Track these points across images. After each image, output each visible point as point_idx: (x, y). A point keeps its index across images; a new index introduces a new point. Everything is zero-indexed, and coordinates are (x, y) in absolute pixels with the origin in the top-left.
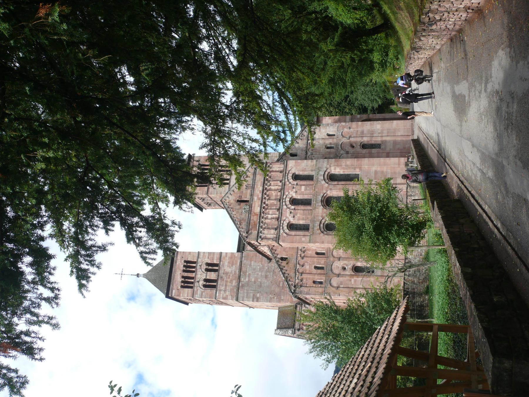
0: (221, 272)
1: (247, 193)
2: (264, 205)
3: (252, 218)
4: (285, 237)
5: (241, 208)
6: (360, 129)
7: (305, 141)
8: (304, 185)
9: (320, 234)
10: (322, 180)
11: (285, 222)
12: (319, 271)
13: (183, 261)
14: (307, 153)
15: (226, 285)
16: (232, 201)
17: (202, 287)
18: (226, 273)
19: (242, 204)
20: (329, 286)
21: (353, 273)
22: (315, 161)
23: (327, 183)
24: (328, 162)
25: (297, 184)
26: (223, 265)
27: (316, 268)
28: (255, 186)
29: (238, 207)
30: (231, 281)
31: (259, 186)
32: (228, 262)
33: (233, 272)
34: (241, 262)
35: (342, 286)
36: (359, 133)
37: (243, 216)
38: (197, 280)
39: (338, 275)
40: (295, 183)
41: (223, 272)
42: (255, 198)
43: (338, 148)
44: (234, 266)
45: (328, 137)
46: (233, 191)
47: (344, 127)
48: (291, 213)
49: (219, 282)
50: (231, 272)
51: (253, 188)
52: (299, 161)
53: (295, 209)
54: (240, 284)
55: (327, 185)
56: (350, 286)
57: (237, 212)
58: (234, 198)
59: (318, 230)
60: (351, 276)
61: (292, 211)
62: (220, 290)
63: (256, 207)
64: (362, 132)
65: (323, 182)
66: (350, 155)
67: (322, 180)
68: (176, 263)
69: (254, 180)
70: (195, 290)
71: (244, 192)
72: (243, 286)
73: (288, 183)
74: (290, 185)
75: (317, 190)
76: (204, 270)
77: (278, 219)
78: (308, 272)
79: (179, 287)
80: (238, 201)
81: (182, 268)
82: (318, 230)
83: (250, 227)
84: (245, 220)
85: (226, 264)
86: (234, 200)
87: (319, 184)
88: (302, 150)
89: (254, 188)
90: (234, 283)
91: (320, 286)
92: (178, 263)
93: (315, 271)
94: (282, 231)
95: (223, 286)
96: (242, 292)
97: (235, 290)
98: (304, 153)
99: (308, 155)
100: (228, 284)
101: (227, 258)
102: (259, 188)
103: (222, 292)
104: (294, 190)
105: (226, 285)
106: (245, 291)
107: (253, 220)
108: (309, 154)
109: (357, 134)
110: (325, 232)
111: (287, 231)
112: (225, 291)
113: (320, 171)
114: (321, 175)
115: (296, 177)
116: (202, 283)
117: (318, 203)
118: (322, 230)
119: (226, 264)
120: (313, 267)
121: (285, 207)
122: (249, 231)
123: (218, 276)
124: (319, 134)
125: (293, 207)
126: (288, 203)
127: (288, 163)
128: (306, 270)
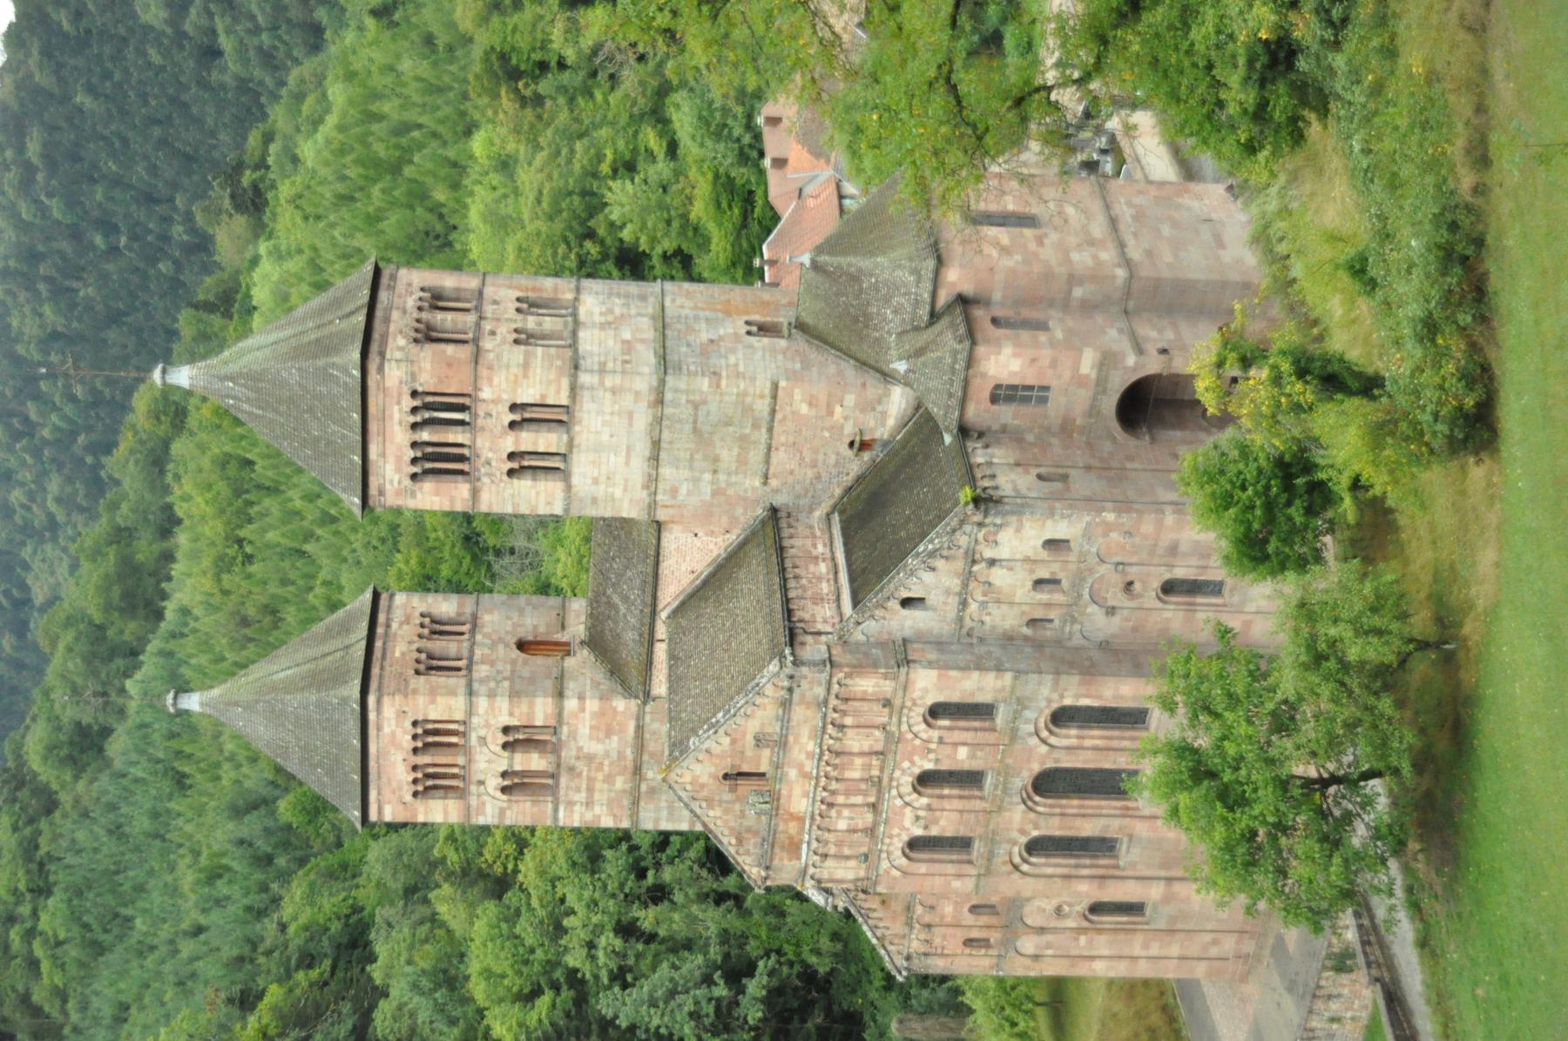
0: (568, 754)
1: (759, 757)
2: (825, 794)
3: (781, 827)
4: (895, 878)
5: (738, 799)
6: (1167, 538)
7: (960, 565)
8: (965, 744)
9: (1009, 873)
10: (1030, 735)
11: (895, 840)
12: (984, 920)
13: (408, 724)
14: (964, 604)
15: (590, 790)
16: (704, 779)
17: (499, 794)
18: (590, 758)
19: (745, 786)
20: (1012, 954)
21: (1085, 924)
22: (1008, 676)
23: (1044, 741)
24: (1056, 683)
25: (941, 741)
26: (573, 735)
27: (974, 909)
28: (791, 738)
29: (727, 796)
30: (609, 779)
31: (804, 739)
32: (592, 728)
33: (614, 755)
34: (640, 729)
35: (1050, 952)
36: (1160, 551)
37: (747, 823)
38: (476, 777)
39: (1042, 930)
40: (935, 734)
41: (574, 753)
42: (793, 773)
43: (1080, 596)
44: (615, 738)
45: (1044, 554)
46: (708, 751)
47: (1108, 528)
48: (918, 818)
49: (563, 781)
50: (607, 754)
51: (782, 743)
52: (953, 673)
53: (929, 808)
54: (644, 787)
55: (1044, 749)
56: (1075, 952)
57: (727, 811)
58: (713, 769)
59: (1004, 863)
60: (1080, 931)
61: (922, 813)
62: (571, 804)
63: (794, 799)
64: (1173, 550)
65: (1034, 741)
66: (1116, 620)
67: (1030, 735)
68: (379, 729)
69: (785, 721)
70: (474, 801)
71: (749, 753)
72: (652, 791)
73: (910, 736)
74: (917, 742)
75: (1009, 761)
76: (498, 749)
77: (871, 832)
78: (948, 920)
79: (408, 798)
80: (726, 777)
81: (407, 742)
82: (1004, 863)
83: (777, 850)
84: (756, 833)
85: (584, 730)
86: (710, 775)
87: (1017, 746)
88: (947, 592)
89: (786, 744)
90: (620, 783)
91: (983, 951)
92: (387, 730)
93: (969, 919)
94: (885, 865)
95: (578, 790)
96: (651, 806)
97: (626, 802)
98: (954, 601)
99: (968, 611)
100: (598, 785)
101: (587, 715)
102: (804, 745)
103: (577, 808)
104: (932, 756)
105: (590, 790)
106: (664, 804)
107: (785, 832)
108: (973, 607)
109: (1152, 552)
110: (1025, 867)
111: (904, 861)
112: (589, 804)
113: (1025, 708)
114: (1027, 721)
115: (935, 712)
116: (494, 783)
117: (1011, 796)
118: (1017, 860)
119: (584, 730)
120: (966, 909)
121: (899, 802)
122: (771, 860)
123: (559, 765)
124: (1015, 543)
125: (924, 801)
126: (907, 789)
127: (912, 676)
128: (942, 917)
